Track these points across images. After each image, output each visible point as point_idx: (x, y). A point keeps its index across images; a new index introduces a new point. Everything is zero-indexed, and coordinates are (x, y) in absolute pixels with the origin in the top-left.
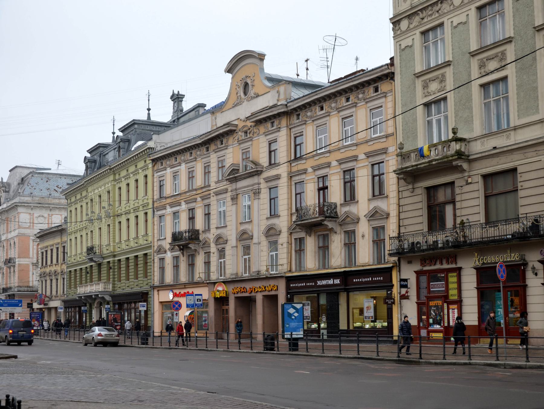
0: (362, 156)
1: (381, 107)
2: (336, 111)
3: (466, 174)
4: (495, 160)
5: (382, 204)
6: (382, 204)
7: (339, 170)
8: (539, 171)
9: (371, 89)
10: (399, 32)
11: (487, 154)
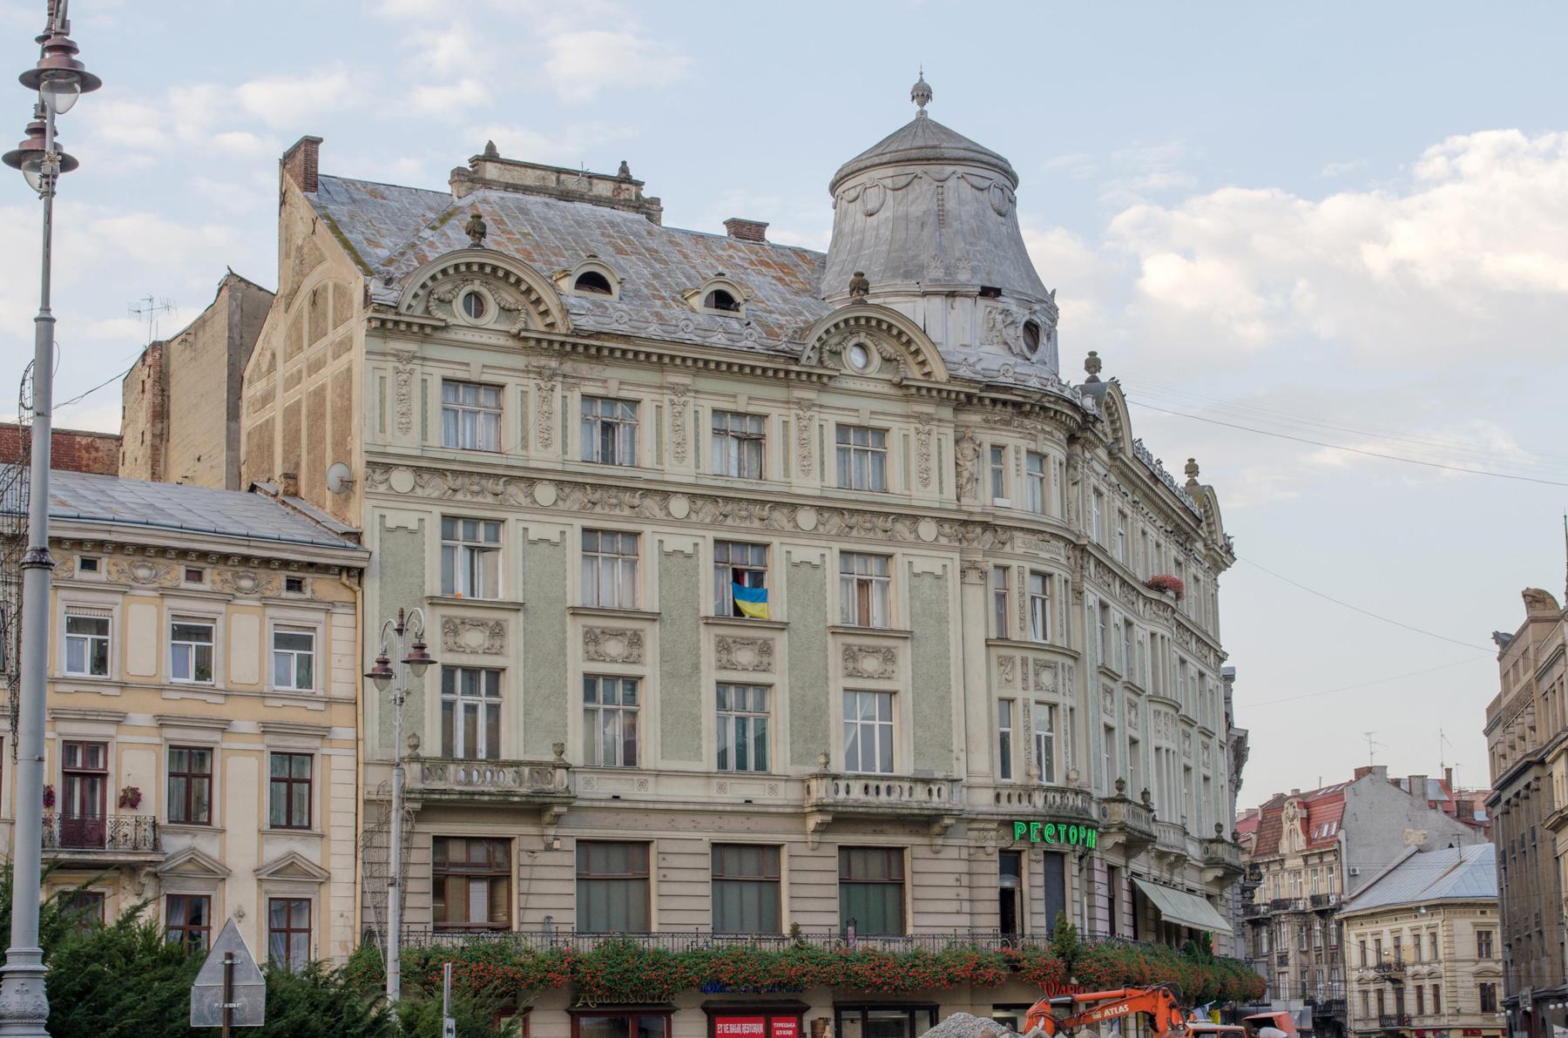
0: (246, 725)
1: (314, 629)
2: (154, 590)
3: (552, 831)
4: (613, 818)
5: (308, 851)
6: (308, 851)
7: (157, 740)
8: (698, 857)
9: (281, 578)
10: (382, 488)
11: (603, 804)
